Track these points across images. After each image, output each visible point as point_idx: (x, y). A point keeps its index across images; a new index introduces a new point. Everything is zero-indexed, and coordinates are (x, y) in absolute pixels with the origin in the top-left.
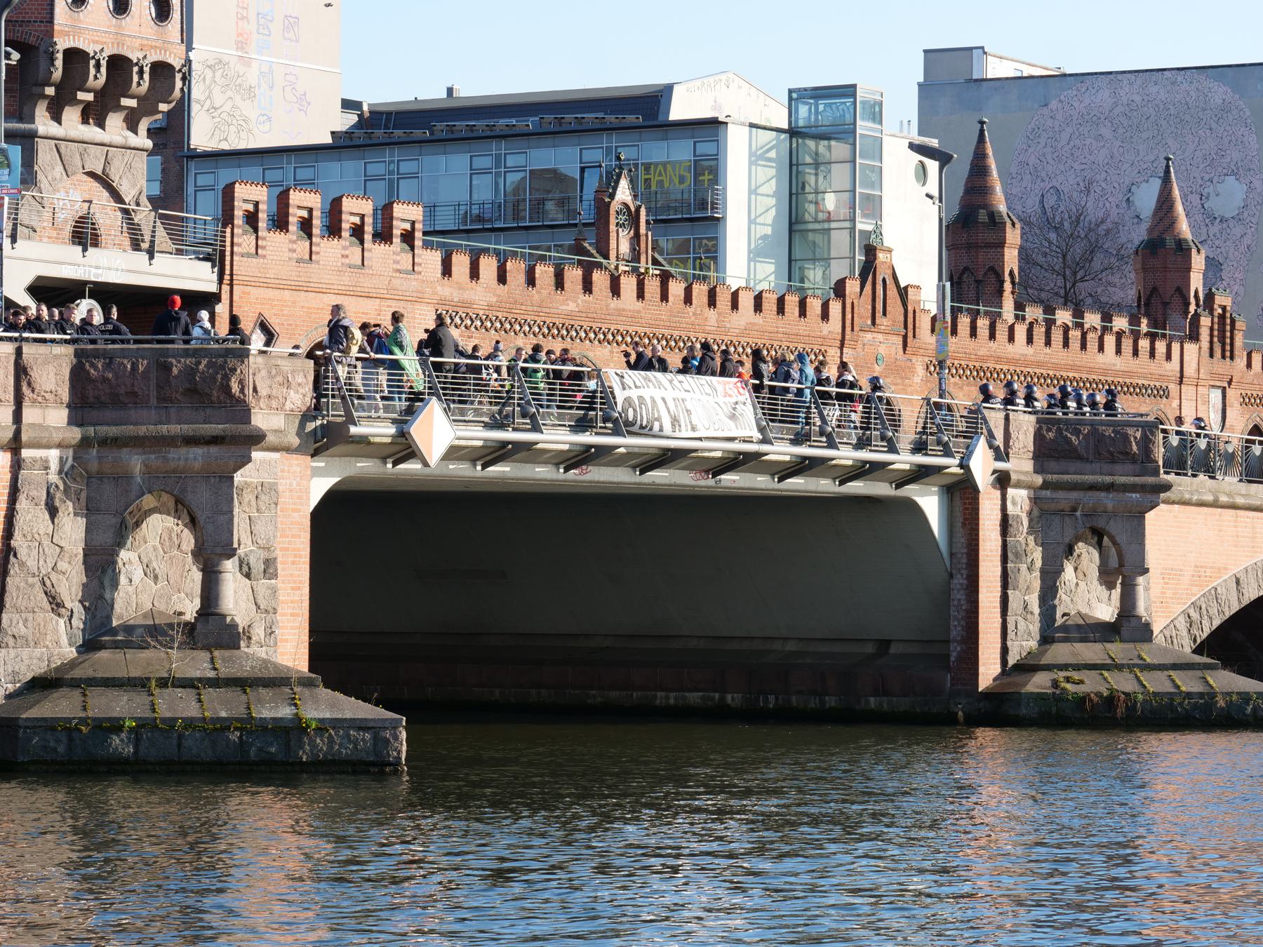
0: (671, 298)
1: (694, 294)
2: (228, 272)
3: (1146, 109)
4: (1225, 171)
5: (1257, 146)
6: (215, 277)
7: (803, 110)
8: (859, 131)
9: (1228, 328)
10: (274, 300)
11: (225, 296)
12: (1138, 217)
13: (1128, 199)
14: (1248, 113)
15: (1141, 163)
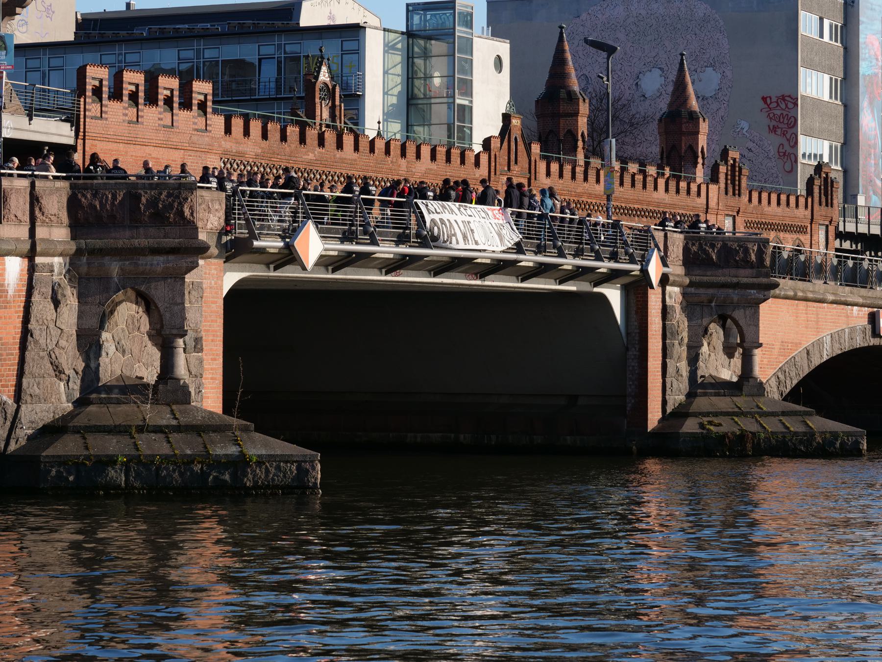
0: (376, 151)
1: (392, 148)
2: (82, 130)
3: (649, 20)
4: (705, 64)
5: (728, 47)
6: (73, 134)
7: (416, 19)
8: (457, 34)
9: (737, 174)
10: (112, 151)
11: (80, 148)
12: (644, 96)
13: (637, 84)
14: (722, 23)
15: (646, 58)
